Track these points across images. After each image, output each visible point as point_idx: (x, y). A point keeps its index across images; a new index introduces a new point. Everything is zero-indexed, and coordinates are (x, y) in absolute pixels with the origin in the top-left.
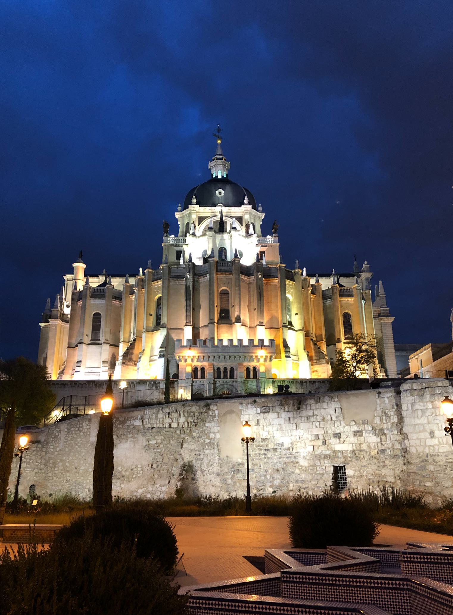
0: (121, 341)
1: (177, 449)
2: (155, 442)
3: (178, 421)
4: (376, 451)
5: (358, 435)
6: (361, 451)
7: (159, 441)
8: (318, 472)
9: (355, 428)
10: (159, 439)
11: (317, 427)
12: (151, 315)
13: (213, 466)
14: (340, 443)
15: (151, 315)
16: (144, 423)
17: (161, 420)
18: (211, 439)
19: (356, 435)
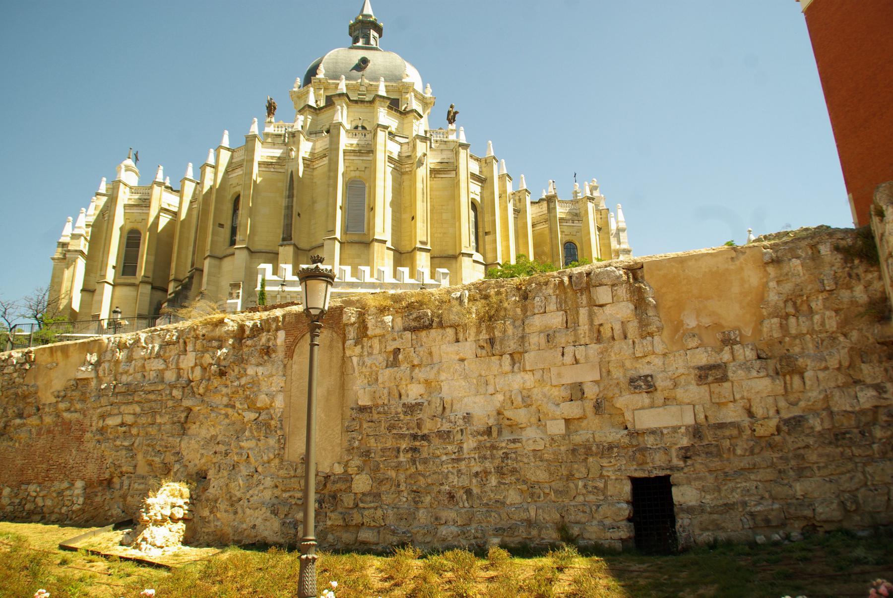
0: (172, 277)
1: (171, 439)
2: (117, 420)
3: (177, 363)
4: (773, 423)
5: (710, 379)
6: (721, 426)
7: (129, 419)
8: (580, 499)
9: (702, 358)
10: (128, 413)
11: (577, 362)
12: (221, 226)
13: (261, 487)
14: (652, 406)
15: (221, 226)
16: (101, 374)
17: (140, 363)
18: (259, 411)
19: (706, 377)
